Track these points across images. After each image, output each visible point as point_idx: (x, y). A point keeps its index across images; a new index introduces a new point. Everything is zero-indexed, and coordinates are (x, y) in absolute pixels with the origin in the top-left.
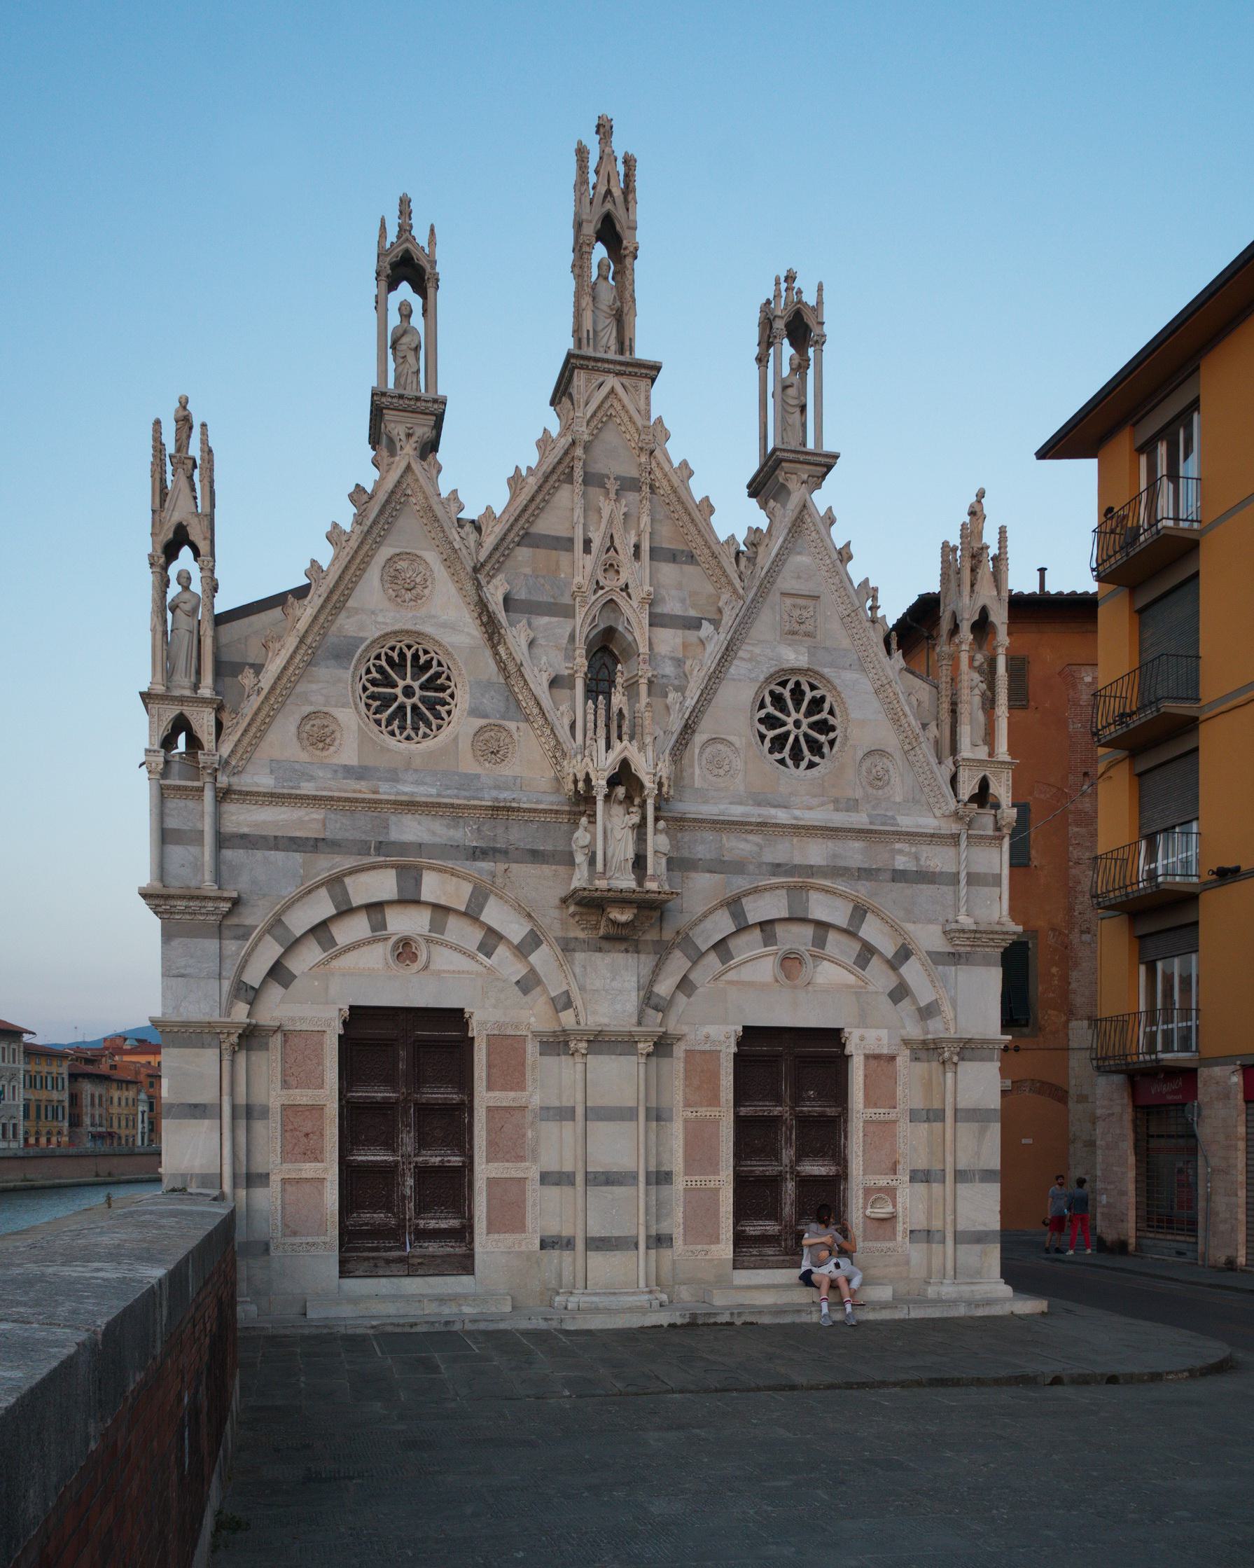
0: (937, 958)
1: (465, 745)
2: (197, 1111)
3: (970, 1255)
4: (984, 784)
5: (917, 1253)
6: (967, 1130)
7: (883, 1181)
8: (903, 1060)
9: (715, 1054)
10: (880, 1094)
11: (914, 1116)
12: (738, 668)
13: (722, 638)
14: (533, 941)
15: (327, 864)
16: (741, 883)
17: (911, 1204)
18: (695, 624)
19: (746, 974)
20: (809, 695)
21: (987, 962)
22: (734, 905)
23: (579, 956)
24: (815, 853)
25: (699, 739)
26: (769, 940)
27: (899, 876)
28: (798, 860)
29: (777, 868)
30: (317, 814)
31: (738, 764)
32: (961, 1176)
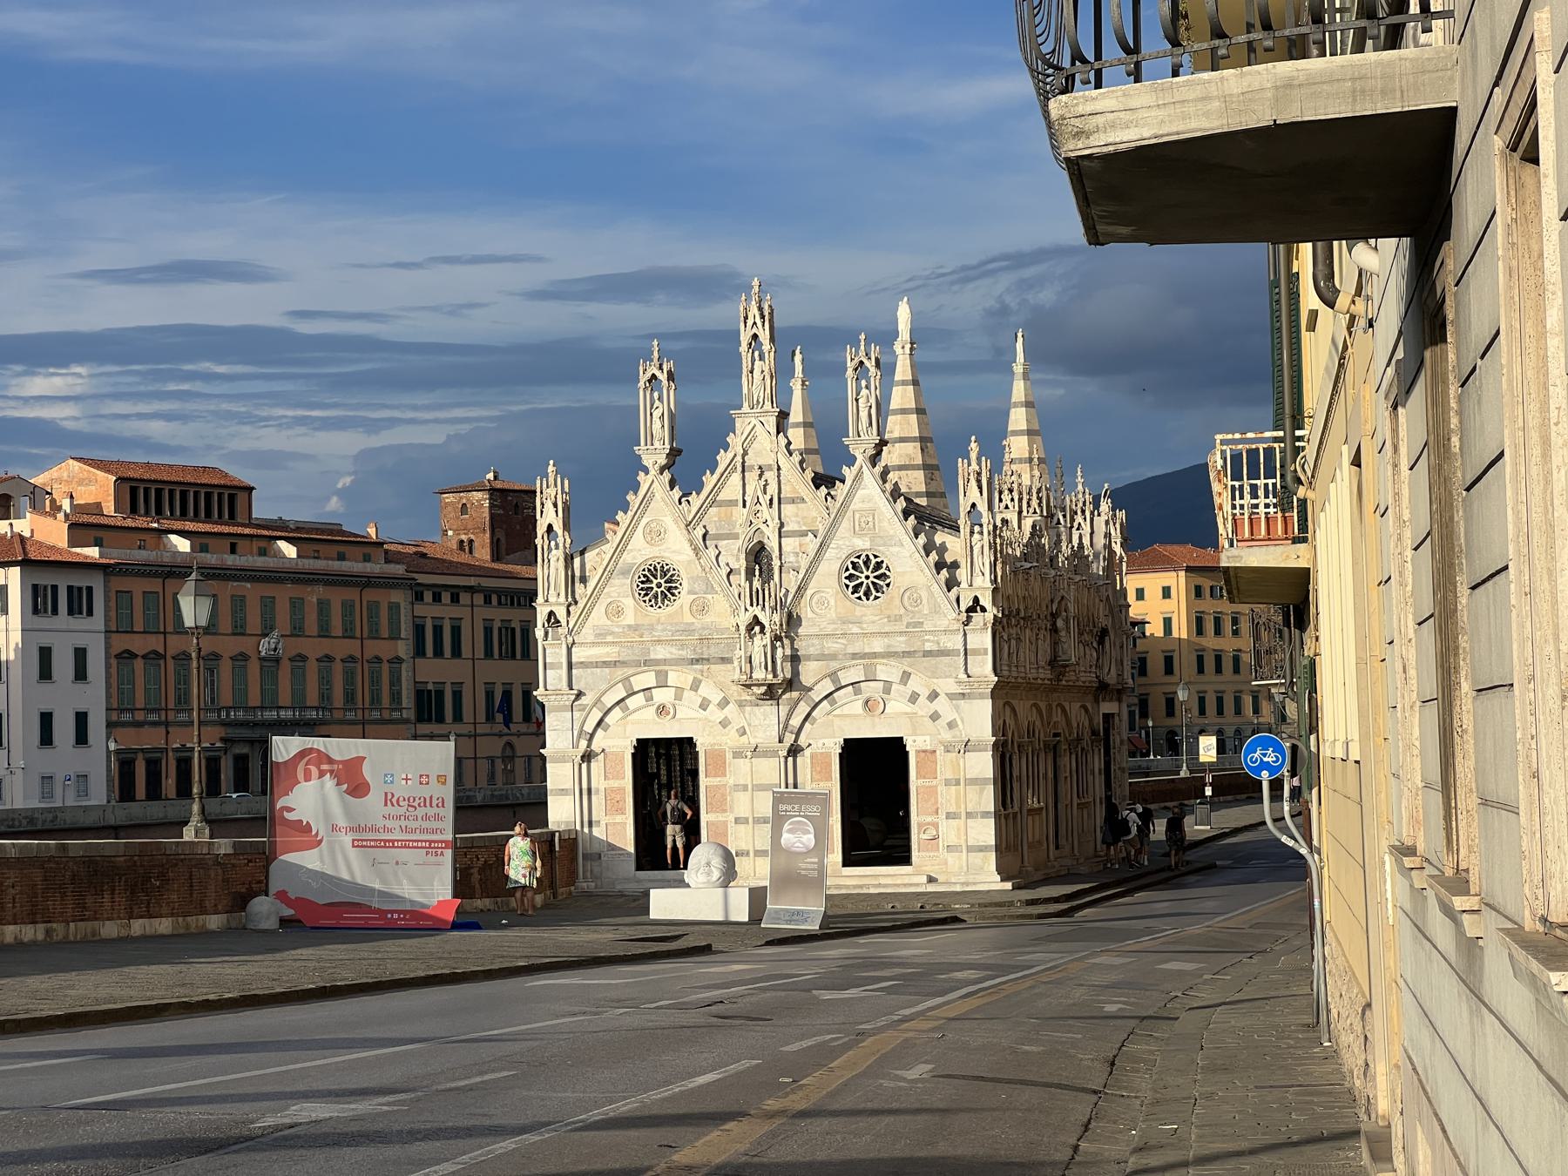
0: (951, 696)
1: (686, 609)
2: (563, 792)
3: (977, 858)
4: (976, 600)
5: (951, 858)
6: (972, 792)
7: (929, 819)
8: (940, 751)
9: (828, 755)
10: (929, 772)
11: (947, 783)
12: (830, 553)
13: (819, 540)
14: (724, 703)
15: (620, 673)
16: (834, 665)
17: (949, 832)
18: (804, 534)
19: (846, 710)
20: (874, 561)
21: (981, 696)
22: (833, 676)
23: (748, 709)
24: (878, 646)
25: (809, 592)
26: (857, 692)
27: (928, 654)
28: (867, 650)
29: (854, 656)
30: (616, 649)
31: (832, 602)
32: (969, 815)
